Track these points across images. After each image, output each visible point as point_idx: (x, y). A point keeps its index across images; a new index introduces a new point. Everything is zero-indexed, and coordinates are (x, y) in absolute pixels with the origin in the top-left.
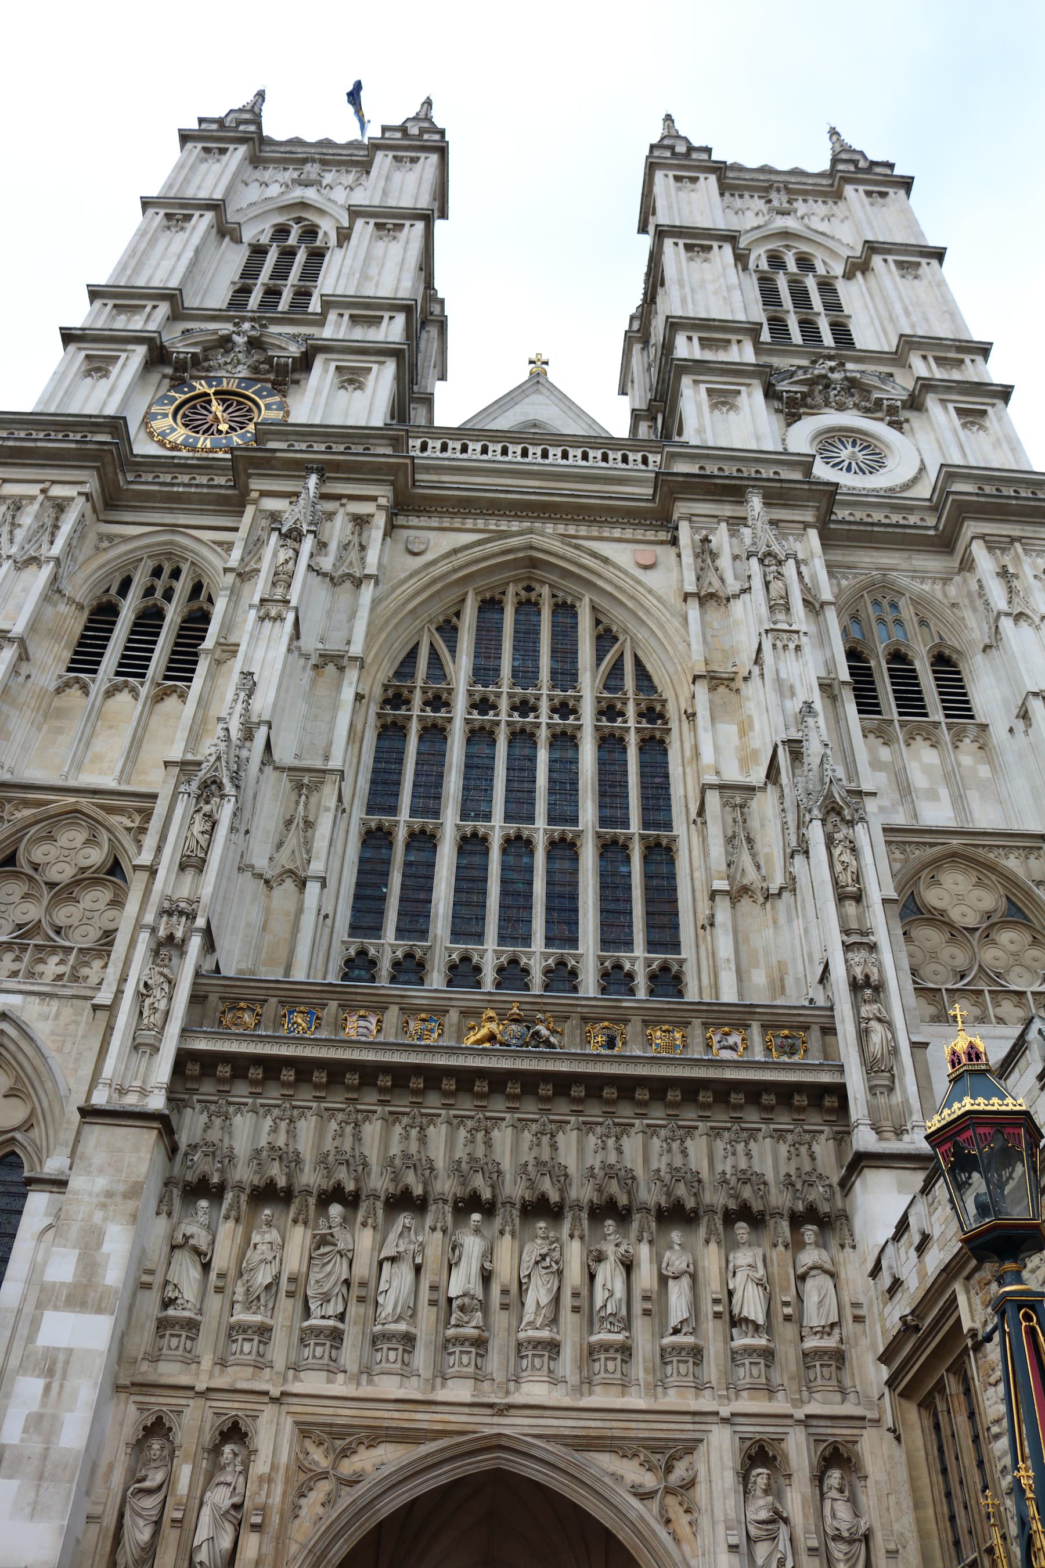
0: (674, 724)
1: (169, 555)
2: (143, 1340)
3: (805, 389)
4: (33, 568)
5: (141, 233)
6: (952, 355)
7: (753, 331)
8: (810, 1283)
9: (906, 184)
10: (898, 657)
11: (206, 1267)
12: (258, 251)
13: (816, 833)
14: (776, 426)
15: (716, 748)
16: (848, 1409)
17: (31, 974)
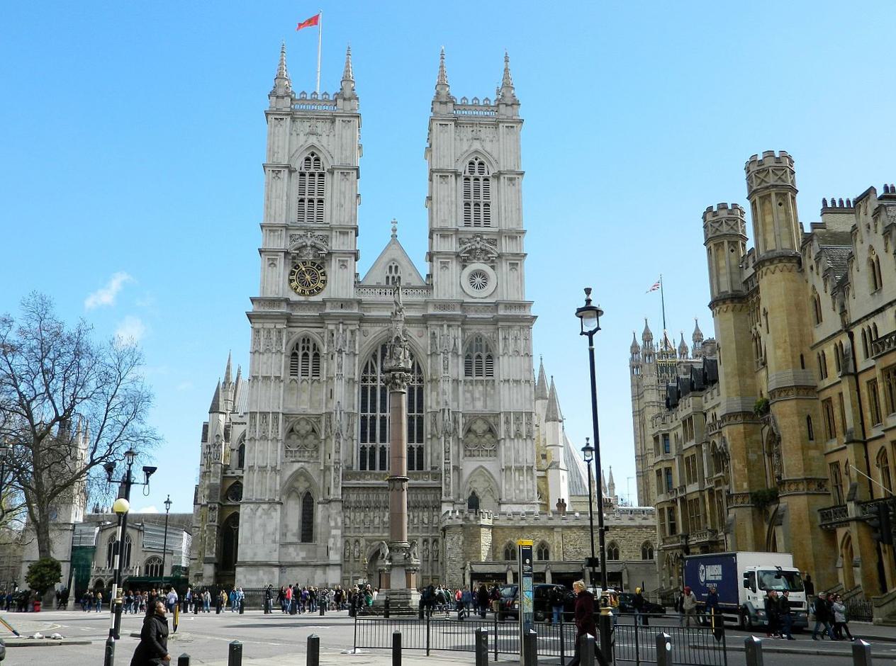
0: (425, 384)
1: (306, 336)
2: (343, 530)
3: (468, 255)
4: (279, 354)
5: (268, 184)
6: (515, 235)
7: (457, 231)
8: (435, 517)
9: (521, 121)
10: (479, 357)
11: (350, 519)
12: (302, 174)
13: (443, 438)
14: (459, 272)
15: (431, 399)
16: (438, 535)
17: (304, 456)
